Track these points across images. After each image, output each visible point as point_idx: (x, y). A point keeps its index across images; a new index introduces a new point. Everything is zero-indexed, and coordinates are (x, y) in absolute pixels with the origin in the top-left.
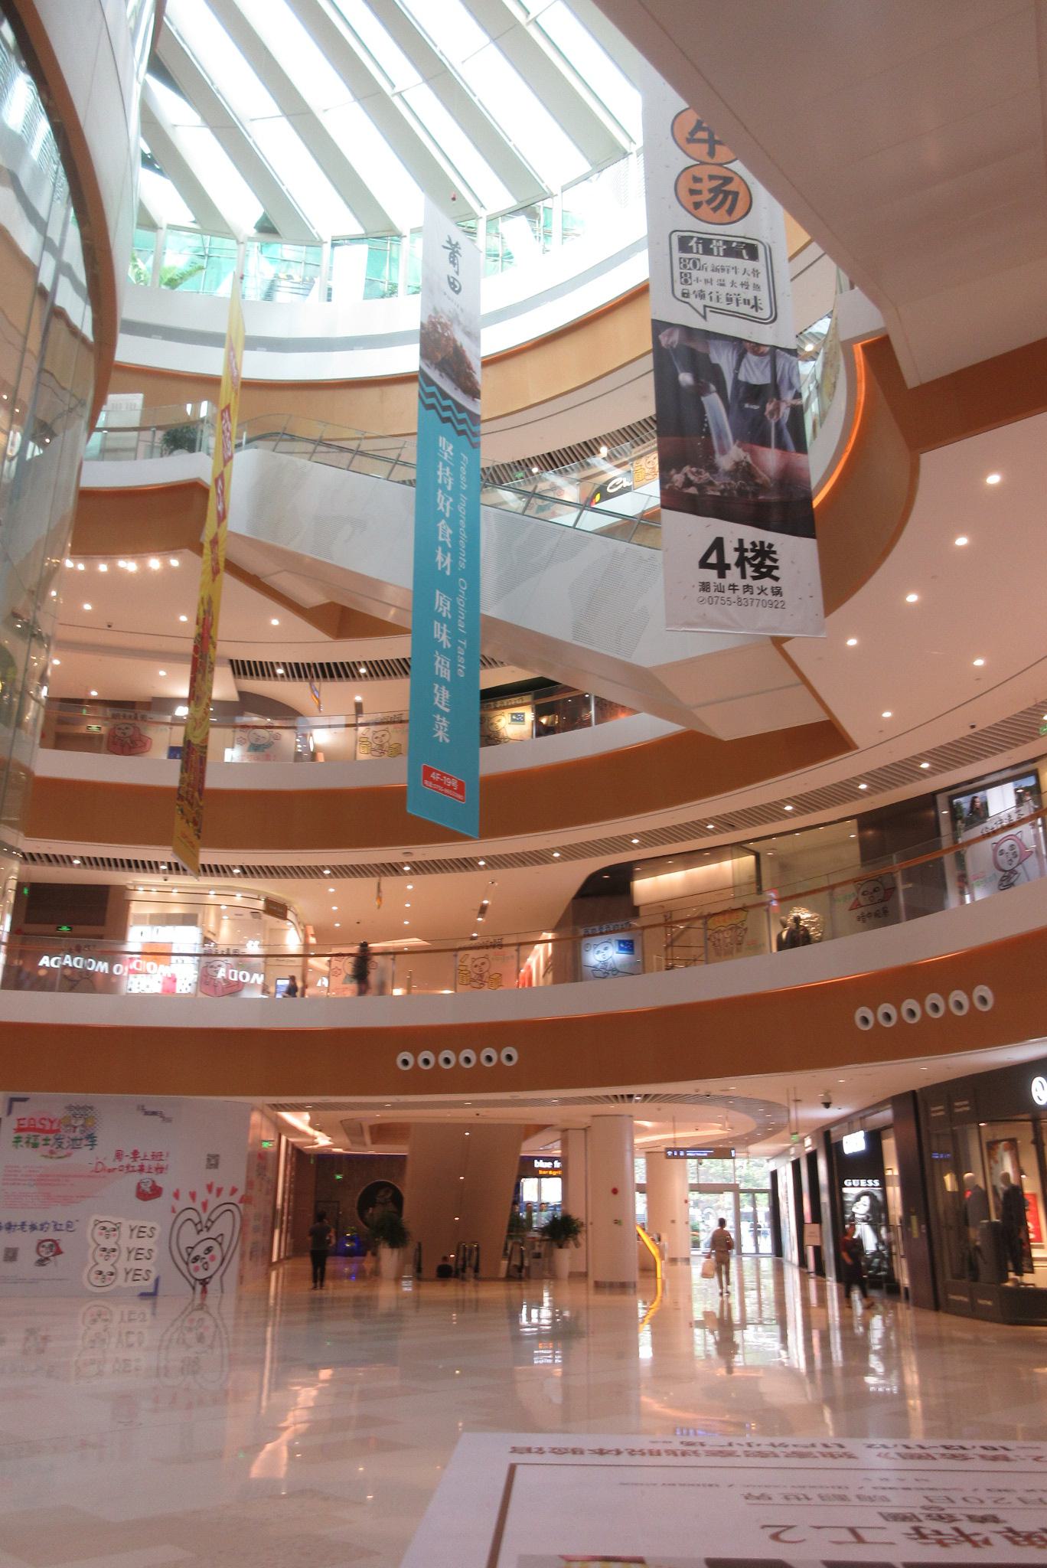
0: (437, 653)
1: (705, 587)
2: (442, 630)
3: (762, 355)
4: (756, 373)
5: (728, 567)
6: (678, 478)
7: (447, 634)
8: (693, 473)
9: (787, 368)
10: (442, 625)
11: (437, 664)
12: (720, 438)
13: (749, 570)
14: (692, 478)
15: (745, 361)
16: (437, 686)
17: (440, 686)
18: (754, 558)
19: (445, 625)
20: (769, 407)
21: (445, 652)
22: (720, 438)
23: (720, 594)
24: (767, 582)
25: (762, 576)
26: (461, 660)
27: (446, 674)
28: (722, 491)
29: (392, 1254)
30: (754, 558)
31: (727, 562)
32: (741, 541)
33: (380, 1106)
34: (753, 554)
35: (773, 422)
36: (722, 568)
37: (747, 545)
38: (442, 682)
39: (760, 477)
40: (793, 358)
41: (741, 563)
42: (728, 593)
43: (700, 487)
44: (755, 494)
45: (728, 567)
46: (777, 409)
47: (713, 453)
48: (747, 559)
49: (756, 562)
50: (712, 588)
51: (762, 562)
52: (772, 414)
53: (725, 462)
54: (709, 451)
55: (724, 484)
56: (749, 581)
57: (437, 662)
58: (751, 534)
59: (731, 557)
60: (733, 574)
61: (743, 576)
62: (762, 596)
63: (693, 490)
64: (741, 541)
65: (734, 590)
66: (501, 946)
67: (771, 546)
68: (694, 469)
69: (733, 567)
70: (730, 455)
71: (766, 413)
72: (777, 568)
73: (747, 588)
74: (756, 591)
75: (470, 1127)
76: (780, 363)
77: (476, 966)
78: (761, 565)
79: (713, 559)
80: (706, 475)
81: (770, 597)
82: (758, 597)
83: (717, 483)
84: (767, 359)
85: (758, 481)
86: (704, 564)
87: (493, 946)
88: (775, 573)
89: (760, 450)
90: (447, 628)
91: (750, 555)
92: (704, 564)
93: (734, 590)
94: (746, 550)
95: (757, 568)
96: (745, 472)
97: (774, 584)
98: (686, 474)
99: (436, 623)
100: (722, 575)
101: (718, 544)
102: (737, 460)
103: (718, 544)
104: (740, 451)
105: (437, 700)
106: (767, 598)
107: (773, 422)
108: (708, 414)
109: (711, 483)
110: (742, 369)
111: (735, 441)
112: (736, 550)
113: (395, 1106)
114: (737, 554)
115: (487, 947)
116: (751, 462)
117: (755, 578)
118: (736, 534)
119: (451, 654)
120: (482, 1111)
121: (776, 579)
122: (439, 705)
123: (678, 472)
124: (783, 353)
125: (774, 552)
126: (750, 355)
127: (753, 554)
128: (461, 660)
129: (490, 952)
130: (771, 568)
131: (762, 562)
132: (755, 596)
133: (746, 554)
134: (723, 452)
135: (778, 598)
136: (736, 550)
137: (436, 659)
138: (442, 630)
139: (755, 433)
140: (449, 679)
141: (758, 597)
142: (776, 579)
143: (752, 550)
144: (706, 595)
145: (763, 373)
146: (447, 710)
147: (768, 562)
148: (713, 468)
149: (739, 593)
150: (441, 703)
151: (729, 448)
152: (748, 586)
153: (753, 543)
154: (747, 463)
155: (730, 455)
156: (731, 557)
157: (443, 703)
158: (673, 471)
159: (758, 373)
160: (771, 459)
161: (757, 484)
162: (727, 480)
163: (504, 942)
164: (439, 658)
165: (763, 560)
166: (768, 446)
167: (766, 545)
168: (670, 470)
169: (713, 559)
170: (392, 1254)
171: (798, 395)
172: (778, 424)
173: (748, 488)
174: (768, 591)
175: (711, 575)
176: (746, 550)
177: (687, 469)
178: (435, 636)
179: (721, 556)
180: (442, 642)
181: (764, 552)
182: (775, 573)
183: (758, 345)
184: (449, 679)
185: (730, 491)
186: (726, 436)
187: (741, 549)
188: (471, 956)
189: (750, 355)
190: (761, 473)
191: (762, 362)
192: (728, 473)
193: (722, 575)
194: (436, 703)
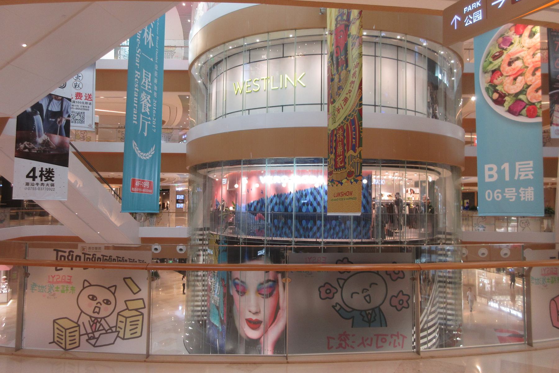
1: (27, 184)
3: (59, 100)
4: (55, 107)
5: (36, 177)
6: (22, 146)
8: (28, 144)
9: (67, 106)
12: (39, 131)
13: (44, 178)
14: (27, 146)
15: (52, 103)
18: (46, 174)
20: (59, 120)
22: (39, 131)
23: (33, 186)
24: (50, 182)
25: (48, 180)
28: (37, 151)
30: (46, 174)
31: (36, 175)
32: (42, 168)
35: (59, 125)
36: (34, 178)
37: (44, 170)
39: (52, 145)
40: (69, 102)
42: (35, 186)
43: (29, 149)
44: (49, 152)
45: (36, 177)
46: (61, 121)
47: (35, 136)
48: (44, 175)
49: (47, 175)
50: (30, 184)
52: (59, 122)
53: (40, 140)
54: (34, 136)
55: (39, 148)
56: (43, 182)
58: (46, 166)
59: (38, 173)
60: (38, 180)
61: (41, 180)
62: (47, 187)
63: (27, 150)
64: (42, 168)
65: (38, 185)
67: (52, 169)
68: (28, 143)
69: (38, 177)
70: (42, 138)
71: (57, 122)
72: (54, 177)
73: (42, 184)
74: (45, 185)
76: (65, 103)
78: (48, 176)
80: (32, 145)
81: (50, 187)
83: (36, 148)
84: (60, 102)
85: (51, 147)
86: (28, 176)
88: (53, 179)
89: (53, 136)
91: (44, 173)
92: (28, 176)
93: (38, 185)
94: (44, 171)
95: (46, 177)
96: (46, 143)
97: (52, 182)
98: (25, 145)
100: (34, 180)
101: (34, 170)
102: (44, 139)
103: (34, 170)
104: (46, 136)
106: (49, 187)
107: (59, 125)
108: (36, 123)
109: (34, 148)
110: (50, 106)
111: (44, 133)
112: (40, 171)
114: (40, 172)
116: (49, 140)
117: (45, 181)
118: (39, 165)
121: (53, 181)
123: (22, 144)
124: (66, 99)
125: (54, 172)
126: (54, 100)
130: (52, 177)
132: (45, 187)
133: (43, 173)
134: (40, 136)
135: (53, 187)
136: (40, 171)
139: (52, 129)
142: (53, 181)
143: (46, 171)
144: (27, 187)
145: (58, 107)
147: (51, 175)
148: (35, 143)
149: (39, 186)
151: (42, 135)
152: (43, 184)
153: (46, 169)
154: (48, 140)
155: (42, 138)
156: (38, 173)
158: (20, 144)
159: (56, 107)
160: (56, 139)
161: (50, 148)
162: (40, 147)
165: (49, 174)
166: (56, 134)
167: (51, 169)
168: (20, 143)
169: (31, 175)
171: (69, 116)
172: (61, 127)
173: (47, 150)
174: (50, 185)
175: (30, 180)
176: (44, 171)
177: (26, 143)
179: (34, 173)
181: (50, 171)
182: (53, 179)
183: (58, 96)
185: (40, 151)
186: (41, 131)
187: (42, 171)
189: (54, 100)
190: (52, 144)
191: (58, 103)
192: (40, 144)
193: (34, 180)
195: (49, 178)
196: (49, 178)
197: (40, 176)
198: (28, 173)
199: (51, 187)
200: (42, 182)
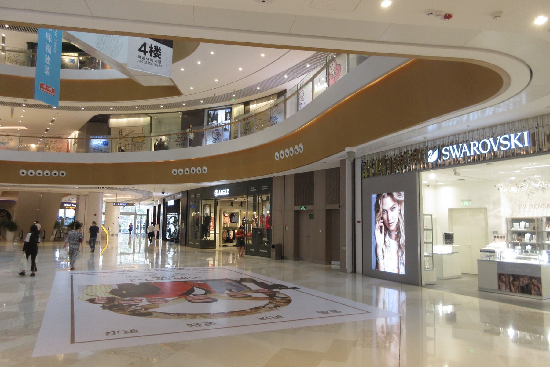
0: (47, 44)
2: (49, 36)
5: (147, 52)
7: (51, 37)
10: (49, 34)
11: (47, 48)
13: (153, 54)
16: (46, 55)
17: (47, 55)
18: (155, 51)
19: (50, 34)
21: (49, 43)
24: (157, 59)
25: (156, 57)
26: (55, 46)
27: (49, 51)
29: (12, 233)
30: (155, 51)
32: (151, 45)
33: (12, 186)
34: (154, 50)
37: (153, 47)
38: (48, 54)
41: (151, 51)
45: (147, 52)
49: (155, 52)
51: (156, 52)
56: (152, 57)
57: (47, 47)
59: (148, 49)
60: (148, 55)
61: (151, 56)
64: (151, 45)
66: (62, 138)
69: (148, 52)
73: (152, 60)
74: (154, 61)
75: (43, 193)
77: (52, 144)
78: (157, 53)
79: (143, 49)
81: (158, 63)
82: (155, 63)
87: (59, 138)
88: (160, 56)
90: (51, 35)
91: (153, 50)
97: (159, 59)
99: (47, 33)
101: (145, 45)
103: (145, 45)
105: (46, 60)
106: (157, 63)
112: (150, 47)
113: (16, 186)
115: (56, 138)
117: (154, 57)
119: (52, 44)
120: (50, 189)
121: (160, 58)
122: (47, 62)
127: (154, 50)
128: (55, 46)
129: (58, 140)
130: (159, 55)
131: (156, 52)
132: (154, 62)
133: (152, 49)
136: (150, 47)
137: (46, 46)
138: (49, 36)
140: (50, 53)
141: (155, 63)
142: (160, 58)
143: (154, 48)
146: (50, 64)
150: (47, 62)
153: (155, 46)
156: (148, 49)
157: (48, 62)
163: (63, 137)
164: (47, 46)
170: (12, 233)
174: (158, 62)
176: (153, 48)
178: (47, 37)
179: (145, 48)
180: (49, 40)
181: (158, 49)
182: (160, 56)
184: (50, 53)
187: (151, 47)
188: (50, 140)
194: (46, 61)
195: (157, 55)
196: (157, 55)
197: (150, 52)
198: (140, 47)
199: (159, 64)
200: (151, 58)
